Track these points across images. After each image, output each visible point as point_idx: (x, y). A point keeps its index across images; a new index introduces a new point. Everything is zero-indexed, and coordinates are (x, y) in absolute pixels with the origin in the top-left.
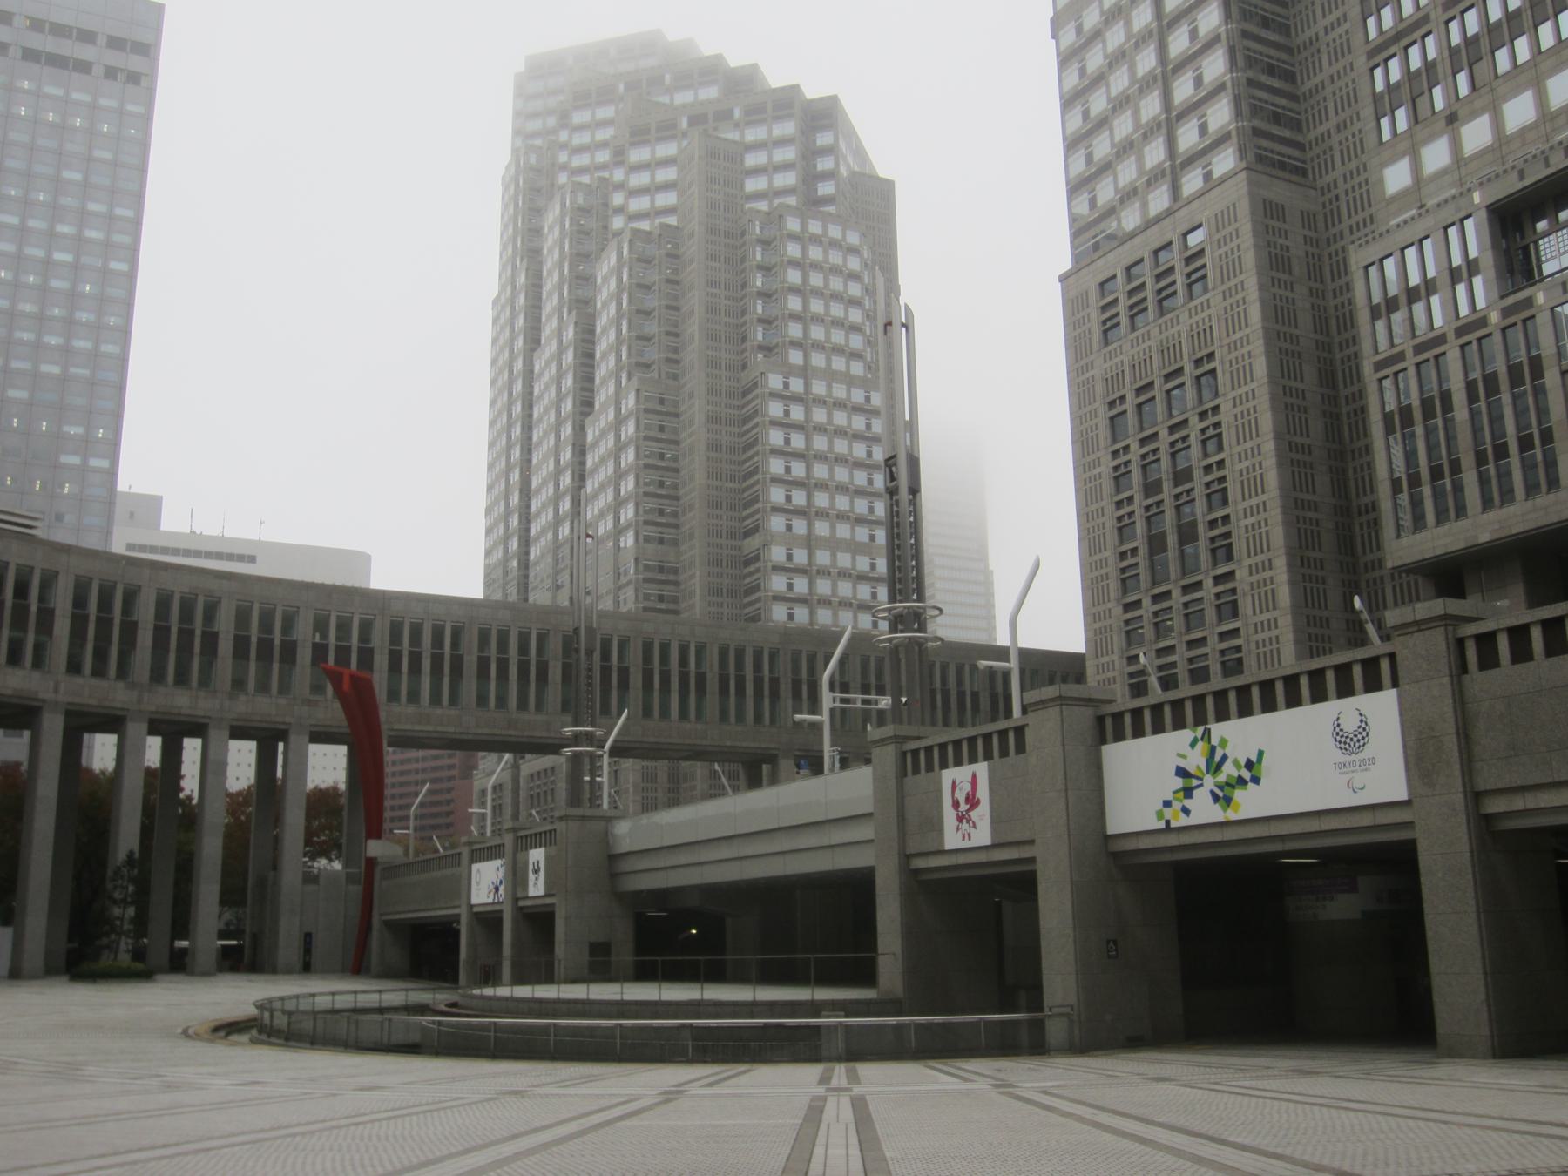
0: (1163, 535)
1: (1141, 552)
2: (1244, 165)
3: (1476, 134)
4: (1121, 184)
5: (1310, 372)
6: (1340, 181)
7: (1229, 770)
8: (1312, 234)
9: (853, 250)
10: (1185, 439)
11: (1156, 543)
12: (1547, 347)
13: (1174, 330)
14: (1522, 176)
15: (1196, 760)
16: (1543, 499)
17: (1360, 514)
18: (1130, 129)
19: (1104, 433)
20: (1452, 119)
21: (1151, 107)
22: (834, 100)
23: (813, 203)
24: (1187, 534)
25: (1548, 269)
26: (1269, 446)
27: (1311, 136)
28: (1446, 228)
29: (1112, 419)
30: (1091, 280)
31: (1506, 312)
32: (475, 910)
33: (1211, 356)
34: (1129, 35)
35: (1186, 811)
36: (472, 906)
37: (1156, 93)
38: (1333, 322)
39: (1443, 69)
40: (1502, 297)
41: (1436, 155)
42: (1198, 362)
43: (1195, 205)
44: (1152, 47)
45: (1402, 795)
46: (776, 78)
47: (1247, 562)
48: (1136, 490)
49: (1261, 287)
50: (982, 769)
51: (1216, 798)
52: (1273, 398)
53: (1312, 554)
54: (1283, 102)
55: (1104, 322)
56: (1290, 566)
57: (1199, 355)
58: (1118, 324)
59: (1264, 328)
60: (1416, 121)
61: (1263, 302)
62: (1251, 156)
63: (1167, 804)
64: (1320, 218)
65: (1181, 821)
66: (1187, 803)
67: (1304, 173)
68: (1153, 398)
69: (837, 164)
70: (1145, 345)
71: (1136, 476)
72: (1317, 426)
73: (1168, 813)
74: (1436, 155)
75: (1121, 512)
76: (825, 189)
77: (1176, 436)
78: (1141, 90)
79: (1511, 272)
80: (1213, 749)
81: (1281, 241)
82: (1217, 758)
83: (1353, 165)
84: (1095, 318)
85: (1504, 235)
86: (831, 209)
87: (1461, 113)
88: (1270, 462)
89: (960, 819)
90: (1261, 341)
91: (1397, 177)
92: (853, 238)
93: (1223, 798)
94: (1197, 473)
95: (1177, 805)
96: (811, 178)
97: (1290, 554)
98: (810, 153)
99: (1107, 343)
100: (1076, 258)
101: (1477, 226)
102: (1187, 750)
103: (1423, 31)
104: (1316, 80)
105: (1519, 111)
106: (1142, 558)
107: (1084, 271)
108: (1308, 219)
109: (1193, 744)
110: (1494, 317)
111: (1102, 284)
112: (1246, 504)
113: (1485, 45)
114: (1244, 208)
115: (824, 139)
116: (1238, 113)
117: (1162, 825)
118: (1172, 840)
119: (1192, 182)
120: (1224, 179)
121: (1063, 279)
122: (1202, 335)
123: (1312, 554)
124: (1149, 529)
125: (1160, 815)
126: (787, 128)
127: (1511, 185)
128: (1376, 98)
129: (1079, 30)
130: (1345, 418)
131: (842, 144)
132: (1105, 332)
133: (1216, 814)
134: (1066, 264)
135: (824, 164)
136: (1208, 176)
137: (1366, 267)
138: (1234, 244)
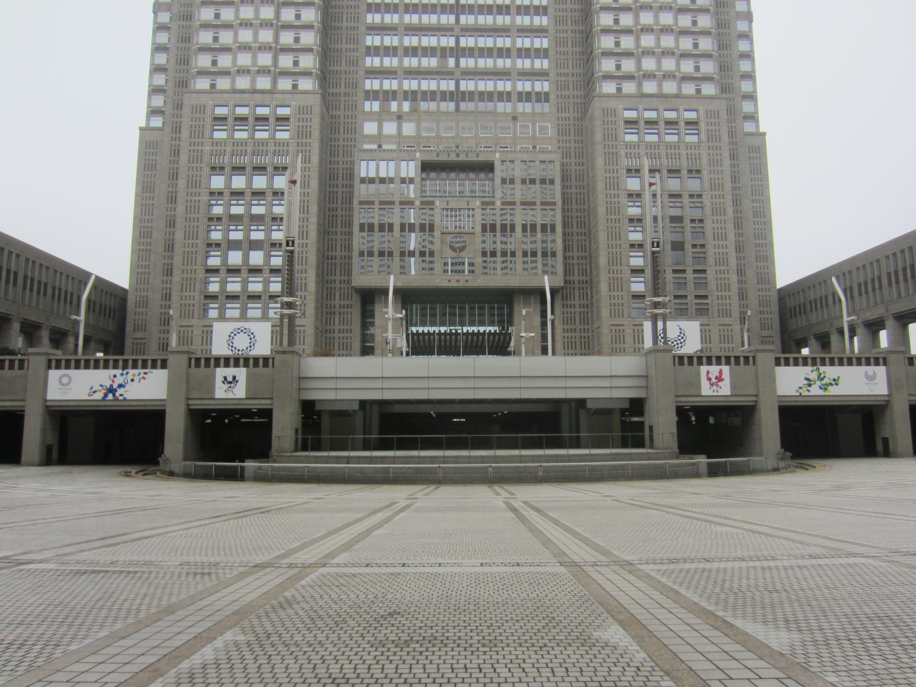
6: (342, 117)
7: (826, 381)
15: (813, 376)
32: (49, 404)
35: (809, 391)
36: (46, 401)
45: (886, 393)
50: (726, 369)
51: (821, 388)
63: (801, 388)
65: (805, 393)
66: (809, 388)
73: (801, 391)
80: (820, 374)
82: (822, 376)
89: (712, 385)
91: (370, 128)
93: (824, 387)
95: (805, 389)
102: (810, 373)
109: (812, 371)
117: (798, 394)
118: (800, 399)
125: (797, 391)
133: (821, 393)
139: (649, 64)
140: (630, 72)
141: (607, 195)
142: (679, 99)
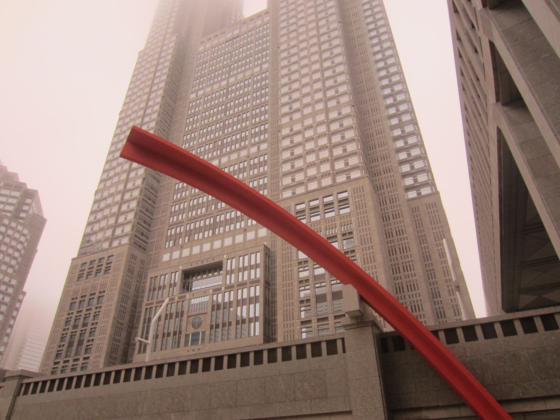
0: (73, 342)
1: (65, 346)
2: (129, 243)
3: (186, 252)
4: (97, 238)
5: (130, 302)
8: (142, 266)
9: (24, 235)
10: (89, 314)
11: (71, 344)
12: (186, 310)
13: (97, 282)
14: (191, 265)
16: (176, 350)
17: (132, 346)
18: (105, 225)
19: (68, 307)
20: (182, 247)
21: (112, 221)
22: (36, 191)
23: (16, 216)
24: (80, 343)
25: (193, 289)
26: (111, 321)
27: (150, 241)
28: (172, 273)
29: (72, 303)
30: (80, 262)
31: (179, 298)
33: (104, 291)
34: (113, 201)
37: (115, 218)
38: (141, 291)
39: (183, 235)
40: (180, 294)
41: (176, 255)
42: (100, 292)
43: (114, 249)
44: (118, 206)
46: (22, 180)
47: (94, 355)
48: (70, 326)
49: (123, 276)
52: (116, 307)
53: (113, 355)
54: (146, 231)
55: (80, 275)
56: (106, 358)
57: (101, 290)
58: (83, 276)
59: (120, 287)
60: (174, 245)
61: (122, 280)
62: (132, 242)
64: (146, 263)
67: (145, 250)
68: (85, 300)
69: (29, 209)
70: (88, 284)
71: (72, 322)
72: (127, 318)
74: (176, 255)
75: (64, 332)
76: (23, 215)
77: (87, 313)
78: (111, 216)
79: (184, 287)
81: (133, 265)
83: (157, 251)
84: (77, 272)
85: (185, 279)
86: (22, 221)
87: (184, 246)
88: (110, 325)
90: (118, 291)
91: (166, 257)
92: (26, 231)
94: (89, 325)
96: (19, 210)
97: (107, 354)
98: (22, 203)
99: (78, 281)
100: (79, 255)
101: (179, 274)
103: (181, 224)
104: (155, 228)
105: (196, 250)
106: (65, 348)
107: (79, 259)
108: (143, 262)
110: (176, 298)
111: (83, 264)
112: (99, 337)
113: (193, 232)
114: (125, 254)
115: (28, 201)
116: (133, 229)
119: (115, 243)
120: (123, 245)
121: (73, 259)
122: (103, 285)
123: (113, 355)
124: (71, 339)
126: (18, 194)
127: (188, 267)
128: (167, 237)
129: (102, 196)
130: (136, 317)
131: (34, 204)
132: (79, 278)
134: (75, 256)
135: (25, 208)
136: (120, 243)
137: (152, 278)
138: (120, 263)
139: (312, 172)
140: (301, 180)
141: (283, 266)
142: (333, 188)
